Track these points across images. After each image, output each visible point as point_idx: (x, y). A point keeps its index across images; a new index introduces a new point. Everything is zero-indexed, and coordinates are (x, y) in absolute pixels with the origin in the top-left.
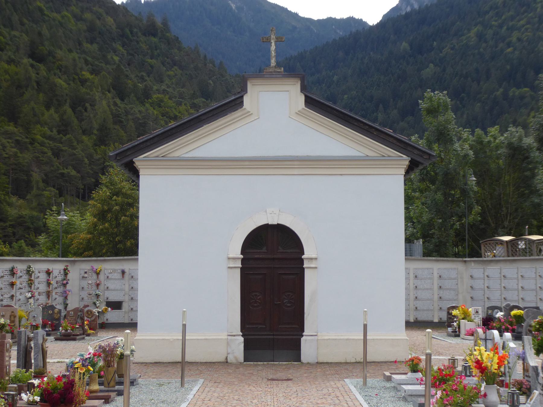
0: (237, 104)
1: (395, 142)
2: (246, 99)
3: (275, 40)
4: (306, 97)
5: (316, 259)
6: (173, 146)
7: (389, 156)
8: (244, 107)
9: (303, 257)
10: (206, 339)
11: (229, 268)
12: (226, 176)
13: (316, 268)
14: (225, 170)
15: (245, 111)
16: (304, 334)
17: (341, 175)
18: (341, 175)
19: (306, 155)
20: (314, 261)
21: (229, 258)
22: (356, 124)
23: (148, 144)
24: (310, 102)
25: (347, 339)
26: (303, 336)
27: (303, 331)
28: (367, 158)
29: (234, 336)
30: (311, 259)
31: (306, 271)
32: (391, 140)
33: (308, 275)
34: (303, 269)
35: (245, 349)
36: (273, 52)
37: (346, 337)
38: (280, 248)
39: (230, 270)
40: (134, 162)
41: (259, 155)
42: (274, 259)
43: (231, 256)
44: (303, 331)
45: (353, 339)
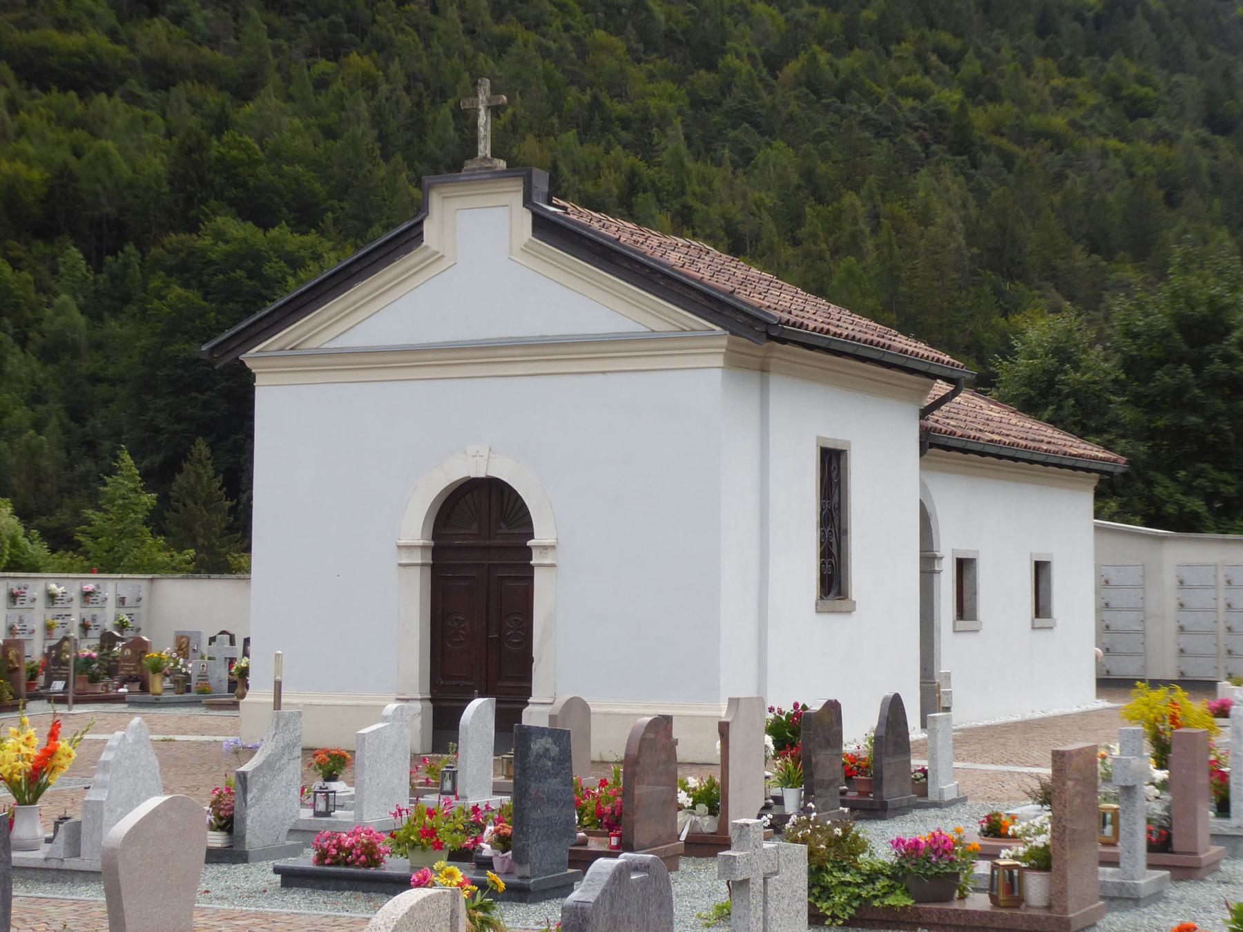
0: (411, 238)
1: (700, 298)
2: (429, 228)
3: (486, 103)
4: (535, 215)
5: (553, 547)
6: (304, 329)
7: (693, 330)
8: (424, 244)
9: (530, 543)
10: (358, 706)
11: (400, 565)
12: (554, 378)
13: (553, 566)
14: (490, 367)
15: (427, 253)
16: (530, 700)
17: (603, 372)
18: (603, 372)
19: (538, 334)
20: (550, 552)
21: (399, 547)
22: (626, 265)
23: (264, 325)
24: (545, 228)
25: (607, 714)
26: (527, 704)
27: (530, 695)
28: (654, 336)
29: (407, 700)
30: (545, 547)
31: (538, 574)
32: (693, 295)
33: (542, 584)
34: (532, 568)
35: (434, 728)
36: (482, 129)
37: (605, 710)
38: (503, 525)
39: (402, 569)
40: (242, 363)
41: (468, 338)
42: (488, 548)
43: (403, 542)
44: (528, 692)
45: (618, 714)
